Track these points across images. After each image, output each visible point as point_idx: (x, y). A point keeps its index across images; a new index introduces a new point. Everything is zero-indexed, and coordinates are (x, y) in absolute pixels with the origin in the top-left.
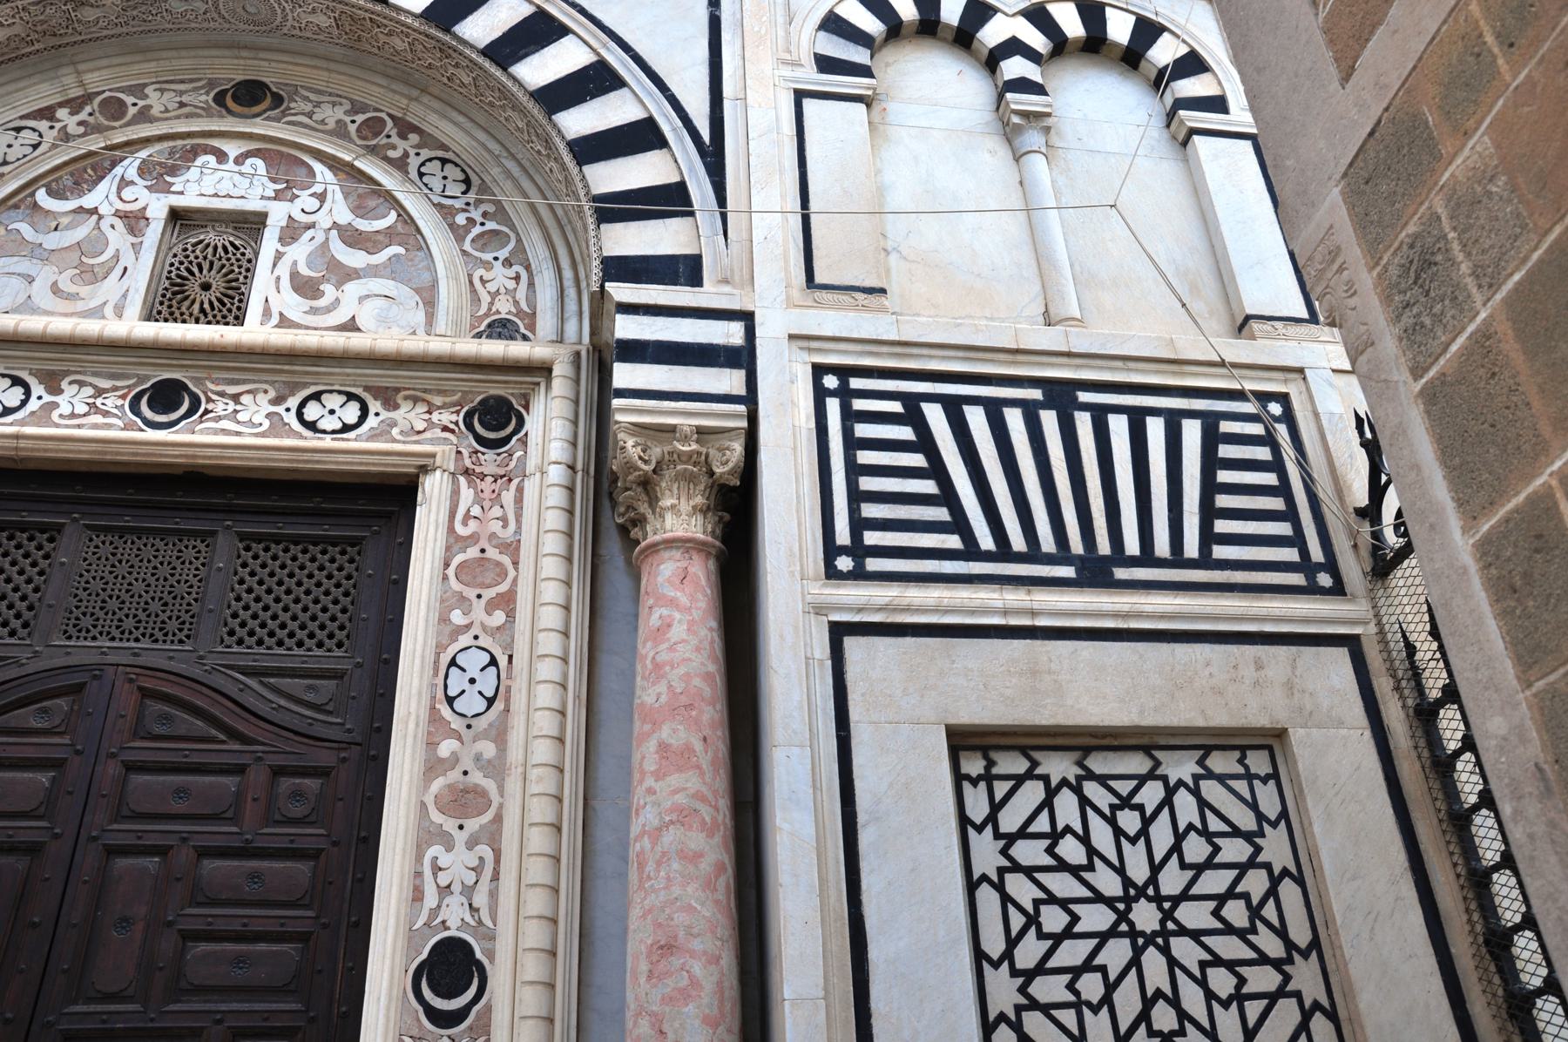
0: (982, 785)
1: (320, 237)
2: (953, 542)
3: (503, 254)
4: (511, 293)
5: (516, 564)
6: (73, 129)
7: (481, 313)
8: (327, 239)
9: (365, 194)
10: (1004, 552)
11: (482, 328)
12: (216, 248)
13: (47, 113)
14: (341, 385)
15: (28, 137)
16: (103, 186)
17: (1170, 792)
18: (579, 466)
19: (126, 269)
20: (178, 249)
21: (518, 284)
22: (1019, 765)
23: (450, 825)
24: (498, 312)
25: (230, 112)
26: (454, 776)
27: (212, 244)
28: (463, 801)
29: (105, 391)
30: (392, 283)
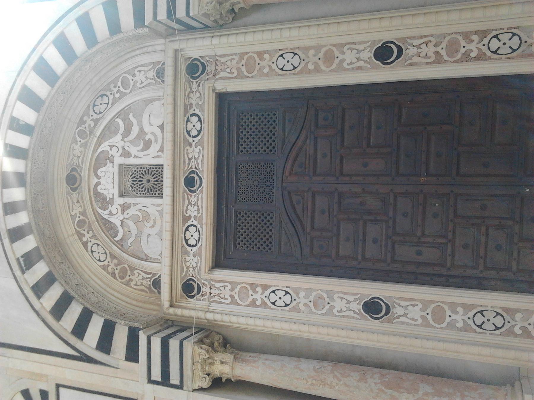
1: (128, 144)
3: (130, 77)
5: (247, 53)
7: (154, 82)
8: (128, 141)
11: (160, 80)
12: (133, 181)
13: (85, 244)
14: (184, 125)
15: (95, 248)
16: (112, 220)
18: (212, 35)
19: (143, 206)
21: (142, 70)
23: (337, 61)
24: (154, 76)
25: (79, 185)
26: (320, 63)
27: (132, 182)
29: (189, 202)
30: (144, 116)
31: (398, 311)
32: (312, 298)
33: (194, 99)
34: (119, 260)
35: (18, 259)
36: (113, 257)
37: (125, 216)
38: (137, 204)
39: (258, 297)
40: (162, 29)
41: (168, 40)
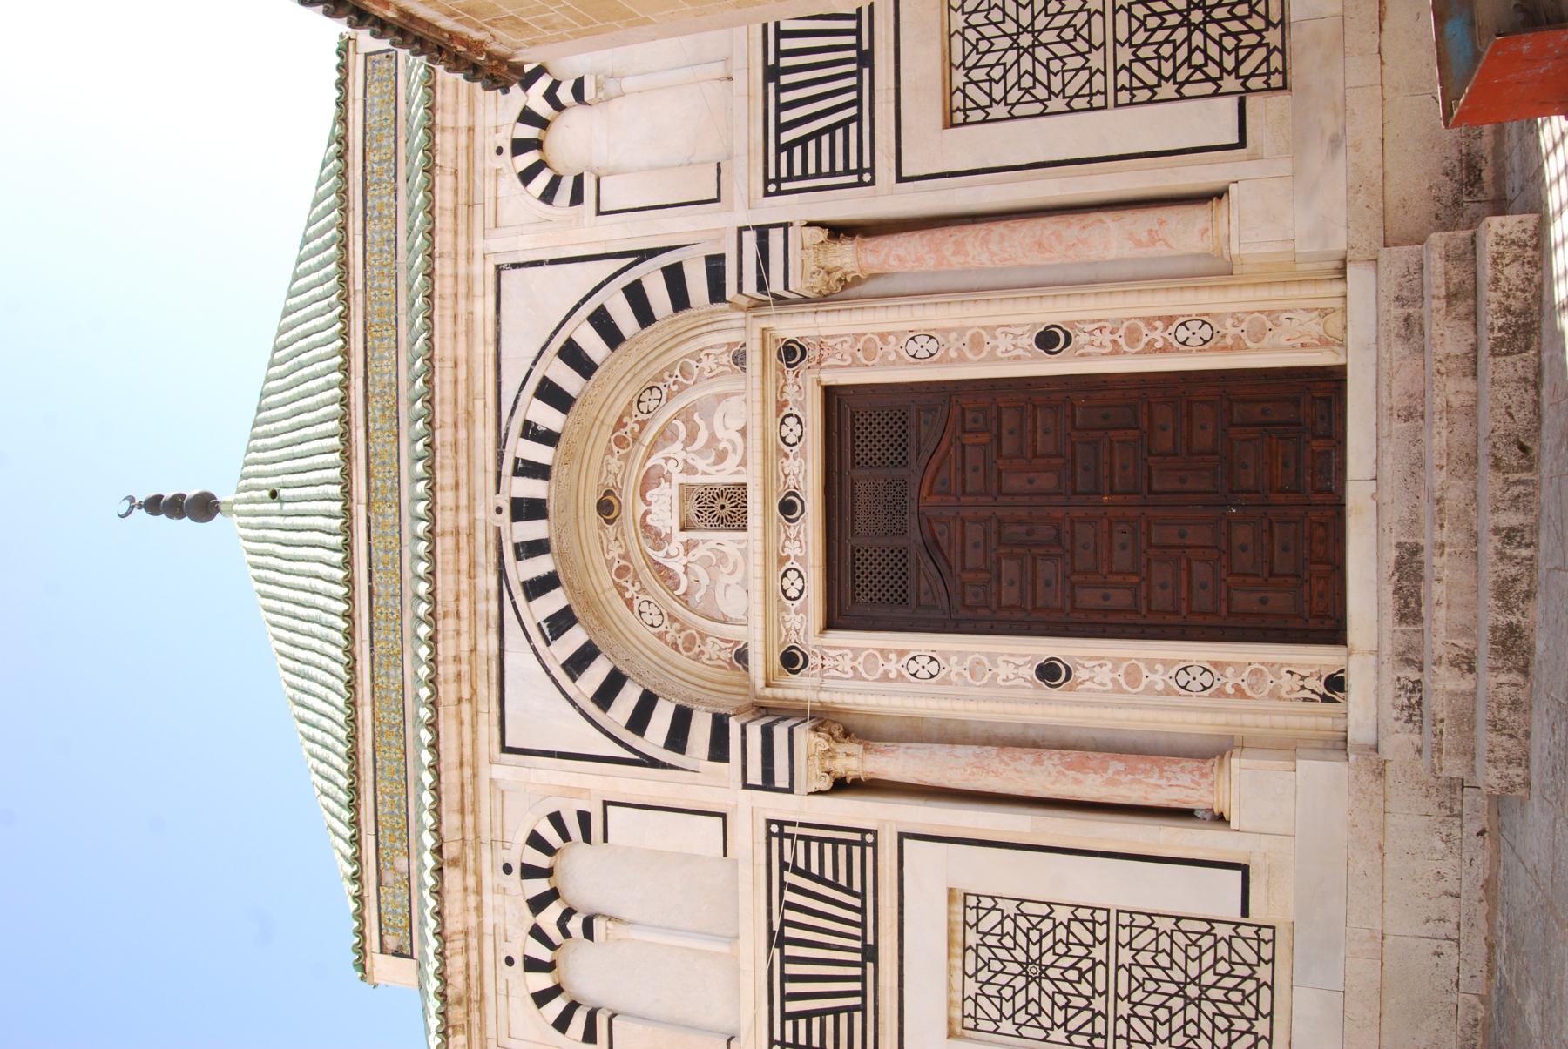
0: (968, 113)
1: (693, 455)
2: (853, 127)
3: (694, 364)
5: (864, 334)
9: (666, 436)
10: (857, 102)
13: (629, 603)
15: (644, 607)
17: (970, 26)
20: (702, 525)
22: (958, 96)
23: (987, 348)
26: (965, 349)
30: (716, 415)
31: (1080, 674)
32: (967, 665)
33: (791, 393)
34: (682, 625)
35: (539, 625)
36: (673, 619)
38: (708, 541)
40: (744, 302)
41: (750, 315)
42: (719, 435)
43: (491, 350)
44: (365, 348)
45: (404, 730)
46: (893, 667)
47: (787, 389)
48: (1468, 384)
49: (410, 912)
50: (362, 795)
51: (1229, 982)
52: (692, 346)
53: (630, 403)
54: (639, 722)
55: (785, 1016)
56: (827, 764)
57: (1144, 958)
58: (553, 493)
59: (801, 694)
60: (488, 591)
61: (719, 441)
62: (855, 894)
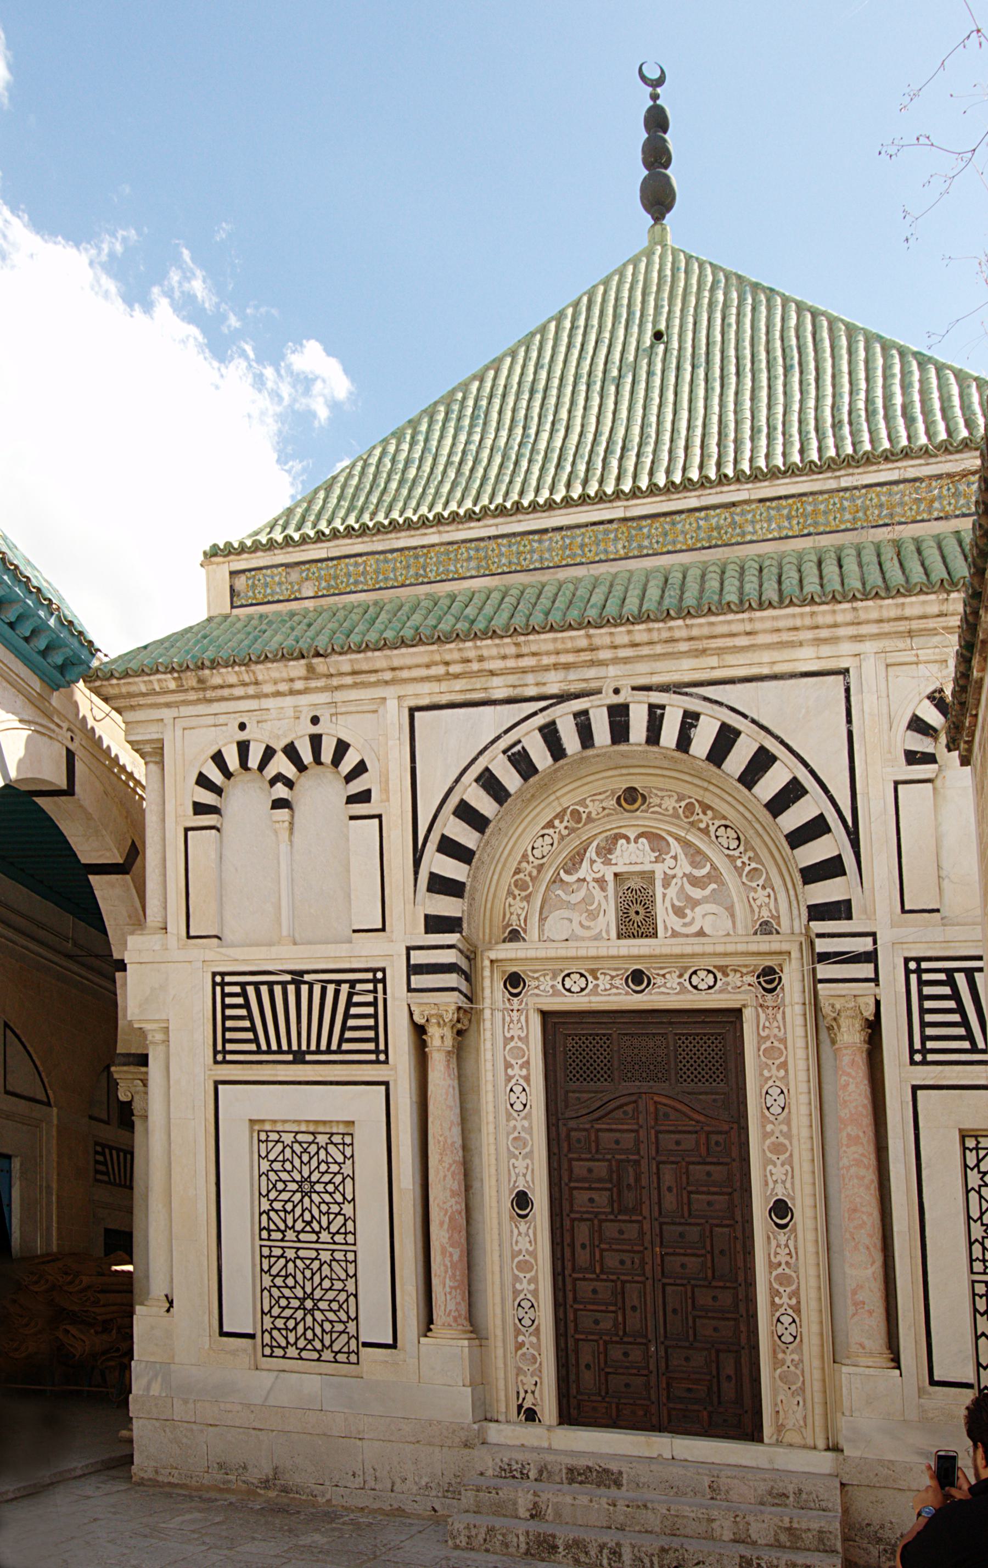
3: (761, 882)
4: (768, 905)
6: (565, 832)
9: (696, 856)
13: (550, 824)
15: (548, 840)
23: (774, 1158)
26: (773, 1139)
28: (778, 1149)
31: (523, 1226)
32: (523, 1134)
33: (734, 979)
34: (536, 877)
35: (519, 742)
36: (540, 868)
37: (592, 884)
39: (515, 1071)
41: (803, 939)
42: (697, 909)
43: (766, 671)
44: (780, 498)
45: (422, 583)
46: (515, 1071)
47: (738, 975)
48: (727, 1535)
49: (269, 603)
50: (360, 540)
51: (318, 1330)
52: (777, 881)
53: (725, 818)
54: (449, 847)
55: (243, 985)
56: (434, 1020)
57: (326, 1270)
58: (636, 748)
59: (487, 992)
60: (544, 684)
61: (692, 910)
62: (339, 1045)
